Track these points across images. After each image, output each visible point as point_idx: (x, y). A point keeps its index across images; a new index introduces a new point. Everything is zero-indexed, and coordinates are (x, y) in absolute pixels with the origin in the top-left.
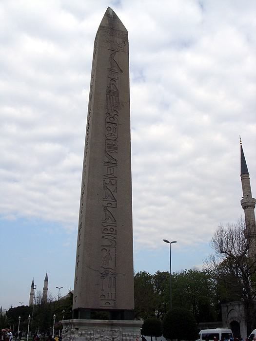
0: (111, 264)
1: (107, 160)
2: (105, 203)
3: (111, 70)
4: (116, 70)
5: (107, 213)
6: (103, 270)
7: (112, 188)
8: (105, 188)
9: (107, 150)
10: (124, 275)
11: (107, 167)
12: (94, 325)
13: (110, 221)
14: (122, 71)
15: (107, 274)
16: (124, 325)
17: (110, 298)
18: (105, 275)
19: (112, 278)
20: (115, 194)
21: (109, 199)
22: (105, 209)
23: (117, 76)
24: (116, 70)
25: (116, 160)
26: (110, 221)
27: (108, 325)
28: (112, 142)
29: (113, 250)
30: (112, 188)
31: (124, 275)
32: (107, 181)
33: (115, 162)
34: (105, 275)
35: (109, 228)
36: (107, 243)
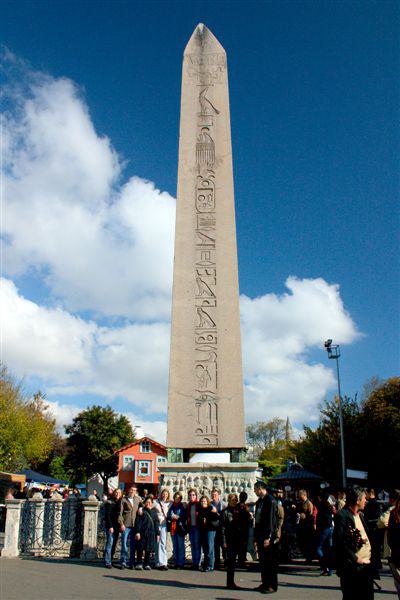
0: (211, 386)
1: (200, 242)
2: (200, 302)
3: (202, 115)
4: (210, 111)
5: (203, 315)
6: (198, 395)
7: (209, 280)
8: (199, 280)
9: (200, 227)
10: (230, 399)
11: (199, 252)
13: (206, 326)
14: (217, 112)
15: (204, 400)
18: (200, 402)
19: (213, 406)
20: (213, 288)
21: (205, 295)
22: (200, 311)
23: (210, 122)
24: (210, 111)
25: (212, 240)
26: (206, 326)
28: (206, 215)
30: (209, 280)
31: (230, 399)
32: (202, 271)
33: (211, 243)
34: (200, 402)
35: (205, 336)
36: (203, 356)
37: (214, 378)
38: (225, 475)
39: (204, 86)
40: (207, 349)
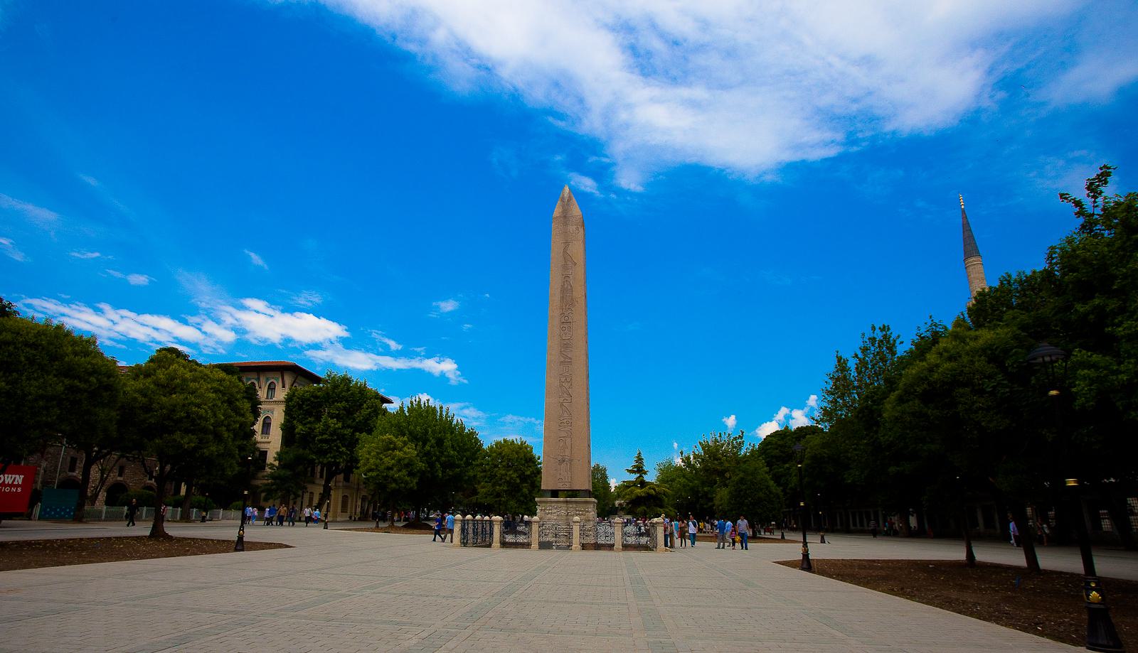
1: (562, 359)
3: (565, 267)
6: (560, 458)
7: (566, 385)
8: (561, 386)
12: (551, 502)
13: (566, 415)
14: (575, 264)
15: (564, 461)
16: (576, 502)
17: (566, 480)
20: (570, 391)
22: (562, 405)
25: (571, 358)
27: (563, 502)
29: (568, 440)
32: (563, 379)
36: (563, 434)
37: (569, 448)
38: (574, 506)
39: (567, 244)
40: (566, 429)
